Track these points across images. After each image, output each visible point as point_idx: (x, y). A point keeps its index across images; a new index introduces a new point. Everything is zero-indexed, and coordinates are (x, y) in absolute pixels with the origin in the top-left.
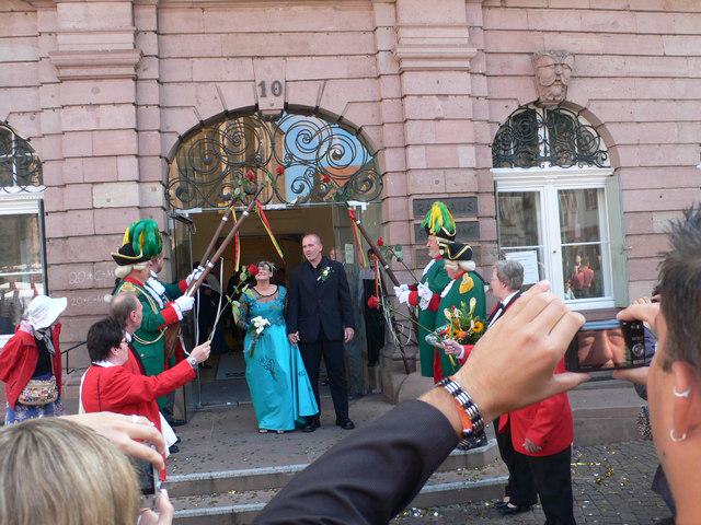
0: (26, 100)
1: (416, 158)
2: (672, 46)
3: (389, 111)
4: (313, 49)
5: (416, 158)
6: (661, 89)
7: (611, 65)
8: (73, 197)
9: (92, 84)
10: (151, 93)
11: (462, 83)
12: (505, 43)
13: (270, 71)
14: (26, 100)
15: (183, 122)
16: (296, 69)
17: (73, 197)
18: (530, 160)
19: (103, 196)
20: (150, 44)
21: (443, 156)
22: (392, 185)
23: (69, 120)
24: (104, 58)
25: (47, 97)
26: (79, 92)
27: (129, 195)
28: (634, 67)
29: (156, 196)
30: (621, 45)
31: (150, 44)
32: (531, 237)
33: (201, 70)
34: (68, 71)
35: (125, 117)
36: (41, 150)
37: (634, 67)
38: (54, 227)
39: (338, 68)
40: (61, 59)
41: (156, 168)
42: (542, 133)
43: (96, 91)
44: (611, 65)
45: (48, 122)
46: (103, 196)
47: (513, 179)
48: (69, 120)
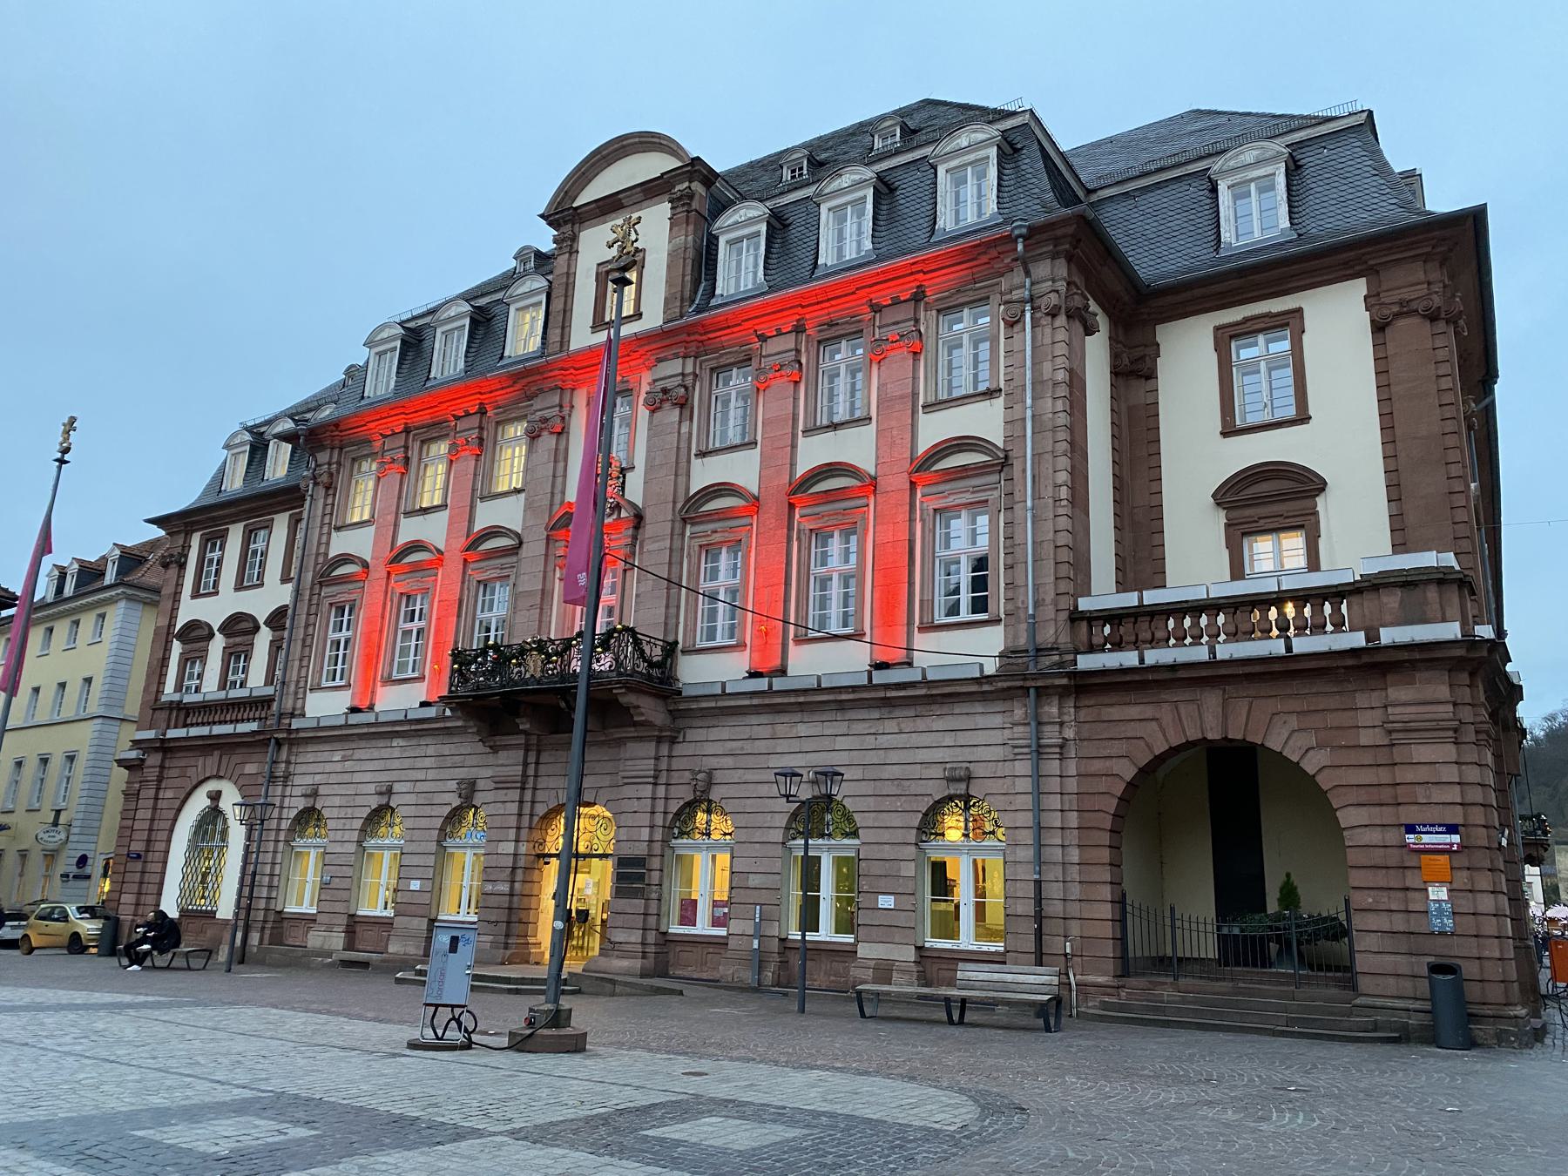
4: (597, 771)
7: (736, 776)
9: (505, 791)
24: (510, 779)
28: (750, 776)
35: (514, 808)
37: (750, 776)
40: (497, 779)
43: (506, 795)
44: (736, 776)
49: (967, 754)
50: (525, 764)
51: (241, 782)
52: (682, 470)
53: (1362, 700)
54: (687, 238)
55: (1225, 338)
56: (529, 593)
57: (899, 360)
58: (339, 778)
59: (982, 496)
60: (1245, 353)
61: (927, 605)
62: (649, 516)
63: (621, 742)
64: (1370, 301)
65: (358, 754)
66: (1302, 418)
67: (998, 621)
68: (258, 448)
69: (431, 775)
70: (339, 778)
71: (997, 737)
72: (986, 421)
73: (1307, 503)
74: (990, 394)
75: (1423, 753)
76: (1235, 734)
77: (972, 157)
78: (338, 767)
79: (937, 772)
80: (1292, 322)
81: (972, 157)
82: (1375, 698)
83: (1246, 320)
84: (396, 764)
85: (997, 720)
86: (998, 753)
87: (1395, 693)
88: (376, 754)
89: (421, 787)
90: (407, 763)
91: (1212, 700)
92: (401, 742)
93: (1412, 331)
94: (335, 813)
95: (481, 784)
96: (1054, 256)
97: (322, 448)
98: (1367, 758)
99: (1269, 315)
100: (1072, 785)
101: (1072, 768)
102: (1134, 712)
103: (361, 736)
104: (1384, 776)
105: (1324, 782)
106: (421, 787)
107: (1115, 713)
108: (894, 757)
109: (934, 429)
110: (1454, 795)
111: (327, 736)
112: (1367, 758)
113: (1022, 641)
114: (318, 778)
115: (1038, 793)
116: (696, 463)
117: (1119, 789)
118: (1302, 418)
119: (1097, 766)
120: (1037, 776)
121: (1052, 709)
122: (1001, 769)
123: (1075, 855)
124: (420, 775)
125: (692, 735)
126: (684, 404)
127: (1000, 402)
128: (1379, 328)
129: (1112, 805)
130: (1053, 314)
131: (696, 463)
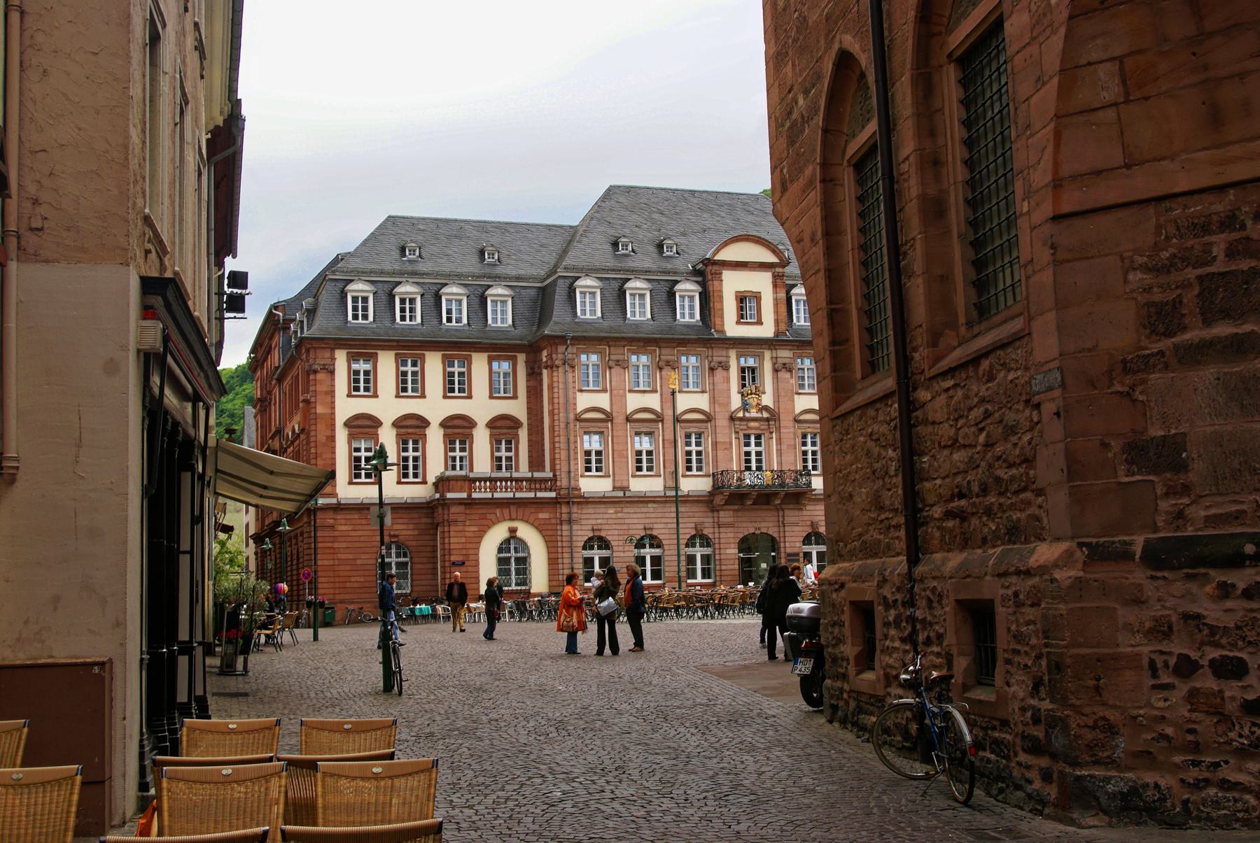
0: (711, 530)
12: (806, 518)
13: (757, 525)
14: (711, 530)
15: (741, 536)
16: (763, 524)
19: (729, 551)
21: (793, 544)
32: (810, 562)
33: (744, 525)
39: (771, 525)
46: (729, 551)
47: (806, 548)
51: (537, 523)
54: (782, 295)
56: (724, 443)
58: (615, 521)
65: (625, 510)
70: (615, 521)
78: (614, 516)
84: (653, 515)
88: (638, 510)
90: (660, 515)
92: (655, 505)
94: (616, 538)
103: (627, 502)
111: (601, 501)
125: (808, 507)
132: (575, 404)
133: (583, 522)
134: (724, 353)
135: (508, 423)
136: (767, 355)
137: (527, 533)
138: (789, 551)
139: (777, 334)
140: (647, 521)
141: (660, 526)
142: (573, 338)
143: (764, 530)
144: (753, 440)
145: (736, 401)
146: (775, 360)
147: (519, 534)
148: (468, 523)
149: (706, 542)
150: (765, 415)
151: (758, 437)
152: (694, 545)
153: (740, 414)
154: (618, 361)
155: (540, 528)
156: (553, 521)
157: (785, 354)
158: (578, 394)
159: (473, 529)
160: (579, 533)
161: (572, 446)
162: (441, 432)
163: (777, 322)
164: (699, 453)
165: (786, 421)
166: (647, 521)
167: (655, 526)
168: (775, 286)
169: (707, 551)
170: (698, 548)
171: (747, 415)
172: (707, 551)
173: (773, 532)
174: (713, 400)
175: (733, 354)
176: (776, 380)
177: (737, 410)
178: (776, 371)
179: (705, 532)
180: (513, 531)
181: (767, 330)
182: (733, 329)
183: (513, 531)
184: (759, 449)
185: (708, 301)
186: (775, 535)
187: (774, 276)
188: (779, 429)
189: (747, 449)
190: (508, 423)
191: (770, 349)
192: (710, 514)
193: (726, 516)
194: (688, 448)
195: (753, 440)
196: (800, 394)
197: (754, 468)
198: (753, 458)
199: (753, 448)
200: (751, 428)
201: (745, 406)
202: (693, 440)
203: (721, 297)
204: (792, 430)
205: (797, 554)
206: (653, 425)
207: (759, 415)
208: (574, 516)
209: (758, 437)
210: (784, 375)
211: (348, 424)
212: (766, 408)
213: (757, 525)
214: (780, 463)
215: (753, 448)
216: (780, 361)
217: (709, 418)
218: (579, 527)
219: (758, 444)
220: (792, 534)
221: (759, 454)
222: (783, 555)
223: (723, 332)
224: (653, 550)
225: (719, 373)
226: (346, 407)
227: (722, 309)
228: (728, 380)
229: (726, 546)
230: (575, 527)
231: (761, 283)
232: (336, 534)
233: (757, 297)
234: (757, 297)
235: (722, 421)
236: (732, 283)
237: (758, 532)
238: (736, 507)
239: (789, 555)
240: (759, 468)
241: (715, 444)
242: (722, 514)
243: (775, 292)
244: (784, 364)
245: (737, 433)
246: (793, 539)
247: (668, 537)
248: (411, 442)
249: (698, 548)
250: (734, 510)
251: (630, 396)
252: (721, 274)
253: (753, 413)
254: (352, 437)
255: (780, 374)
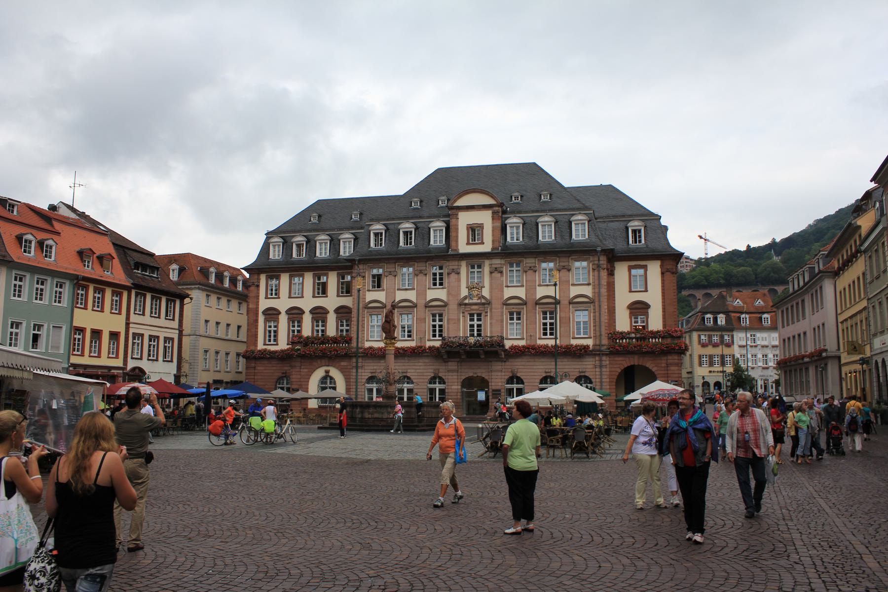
0: (444, 374)
1: (493, 384)
2: (535, 367)
3: (490, 377)
5: (493, 384)
6: (532, 374)
8: (449, 387)
10: (459, 374)
11: (500, 374)
12: (508, 367)
15: (463, 378)
16: (478, 371)
17: (449, 387)
18: (512, 383)
19: (453, 387)
20: (460, 367)
22: (490, 387)
23: (450, 377)
25: (447, 374)
26: (450, 374)
27: (456, 387)
29: (460, 387)
30: (526, 367)
31: (460, 367)
34: (449, 371)
36: (446, 381)
38: (447, 391)
41: (460, 384)
42: (515, 380)
44: (525, 370)
45: (447, 377)
46: (453, 387)
48: (450, 377)
49: (584, 366)
50: (458, 366)
52: (502, 291)
53: (663, 358)
54: (498, 224)
55: (630, 268)
57: (564, 272)
59: (587, 309)
60: (634, 272)
61: (573, 333)
62: (493, 302)
63: (491, 361)
64: (661, 266)
66: (646, 291)
67: (591, 338)
68: (287, 244)
69: (421, 367)
71: (591, 363)
72: (588, 291)
73: (646, 310)
74: (589, 284)
75: (673, 368)
76: (640, 364)
77: (582, 222)
79: (578, 370)
80: (645, 267)
81: (582, 222)
82: (665, 358)
83: (636, 265)
85: (591, 359)
86: (592, 366)
87: (669, 357)
89: (418, 371)
91: (636, 357)
93: (668, 274)
95: (441, 370)
96: (604, 255)
97: (360, 264)
98: (663, 369)
99: (640, 265)
100: (608, 373)
101: (608, 370)
102: (620, 359)
104: (666, 372)
105: (656, 373)
106: (418, 371)
107: (617, 359)
108: (567, 367)
109: (574, 291)
110: (677, 375)
112: (663, 369)
113: (598, 343)
114: (375, 367)
115: (601, 375)
116: (505, 289)
117: (617, 374)
118: (646, 291)
119: (613, 369)
120: (601, 372)
121: (604, 358)
122: (592, 370)
123: (608, 387)
124: (418, 368)
126: (501, 272)
127: (590, 287)
128: (662, 273)
129: (616, 377)
130: (604, 269)
131: (505, 289)
132: (365, 298)
133: (366, 368)
134: (456, 263)
135: (346, 310)
136: (487, 263)
137: (335, 373)
138: (494, 388)
139: (493, 249)
140: (403, 367)
141: (413, 371)
142: (360, 261)
143: (479, 375)
144: (475, 317)
145: (464, 292)
146: (491, 265)
147: (331, 374)
148: (302, 367)
149: (442, 381)
150: (483, 301)
151: (479, 315)
152: (435, 383)
153: (467, 301)
154: (390, 272)
155: (342, 370)
156: (349, 367)
157: (497, 262)
158: (367, 292)
159: (306, 370)
160: (363, 374)
161: (360, 323)
162: (311, 316)
163: (493, 241)
164: (440, 326)
165: (496, 305)
166: (403, 367)
167: (409, 371)
168: (493, 219)
169: (442, 386)
170: (437, 385)
171: (471, 301)
172: (442, 386)
173: (485, 375)
174: (449, 294)
175: (464, 264)
176: (491, 278)
177: (465, 298)
178: (491, 273)
179: (440, 375)
180: (327, 372)
181: (487, 247)
182: (463, 247)
183: (327, 372)
184: (479, 323)
185: (449, 232)
186: (486, 378)
187: (493, 213)
188: (491, 310)
189: (472, 323)
190: (346, 310)
191: (488, 259)
192: (444, 364)
193: (452, 365)
194: (441, 323)
195: (475, 317)
196: (508, 287)
197: (476, 335)
198: (475, 328)
199: (476, 323)
200: (473, 310)
201: (470, 296)
202: (437, 318)
203: (457, 229)
204: (500, 310)
205: (499, 390)
206: (411, 309)
207: (479, 301)
208: (360, 364)
209: (479, 315)
210: (497, 275)
211: (264, 313)
212: (483, 297)
213: (475, 371)
214: (491, 332)
215: (476, 323)
216: (494, 266)
217: (446, 305)
218: (363, 371)
219: (479, 320)
220: (496, 377)
221: (479, 326)
222: (490, 390)
223: (457, 250)
224: (408, 385)
225: (453, 276)
226: (264, 304)
227: (457, 237)
228: (459, 280)
229: (451, 384)
230: (360, 370)
231: (485, 218)
232: (256, 371)
233: (481, 226)
234: (481, 226)
235: (453, 306)
236: (464, 220)
237: (475, 375)
238: (458, 360)
239: (493, 390)
240: (479, 335)
241: (448, 320)
242: (450, 363)
243: (493, 223)
244: (496, 268)
245: (463, 313)
246: (497, 380)
247: (416, 377)
248: (296, 322)
249: (437, 385)
250: (458, 362)
251: (398, 292)
252: (457, 215)
253: (475, 300)
254: (266, 321)
255: (493, 274)
